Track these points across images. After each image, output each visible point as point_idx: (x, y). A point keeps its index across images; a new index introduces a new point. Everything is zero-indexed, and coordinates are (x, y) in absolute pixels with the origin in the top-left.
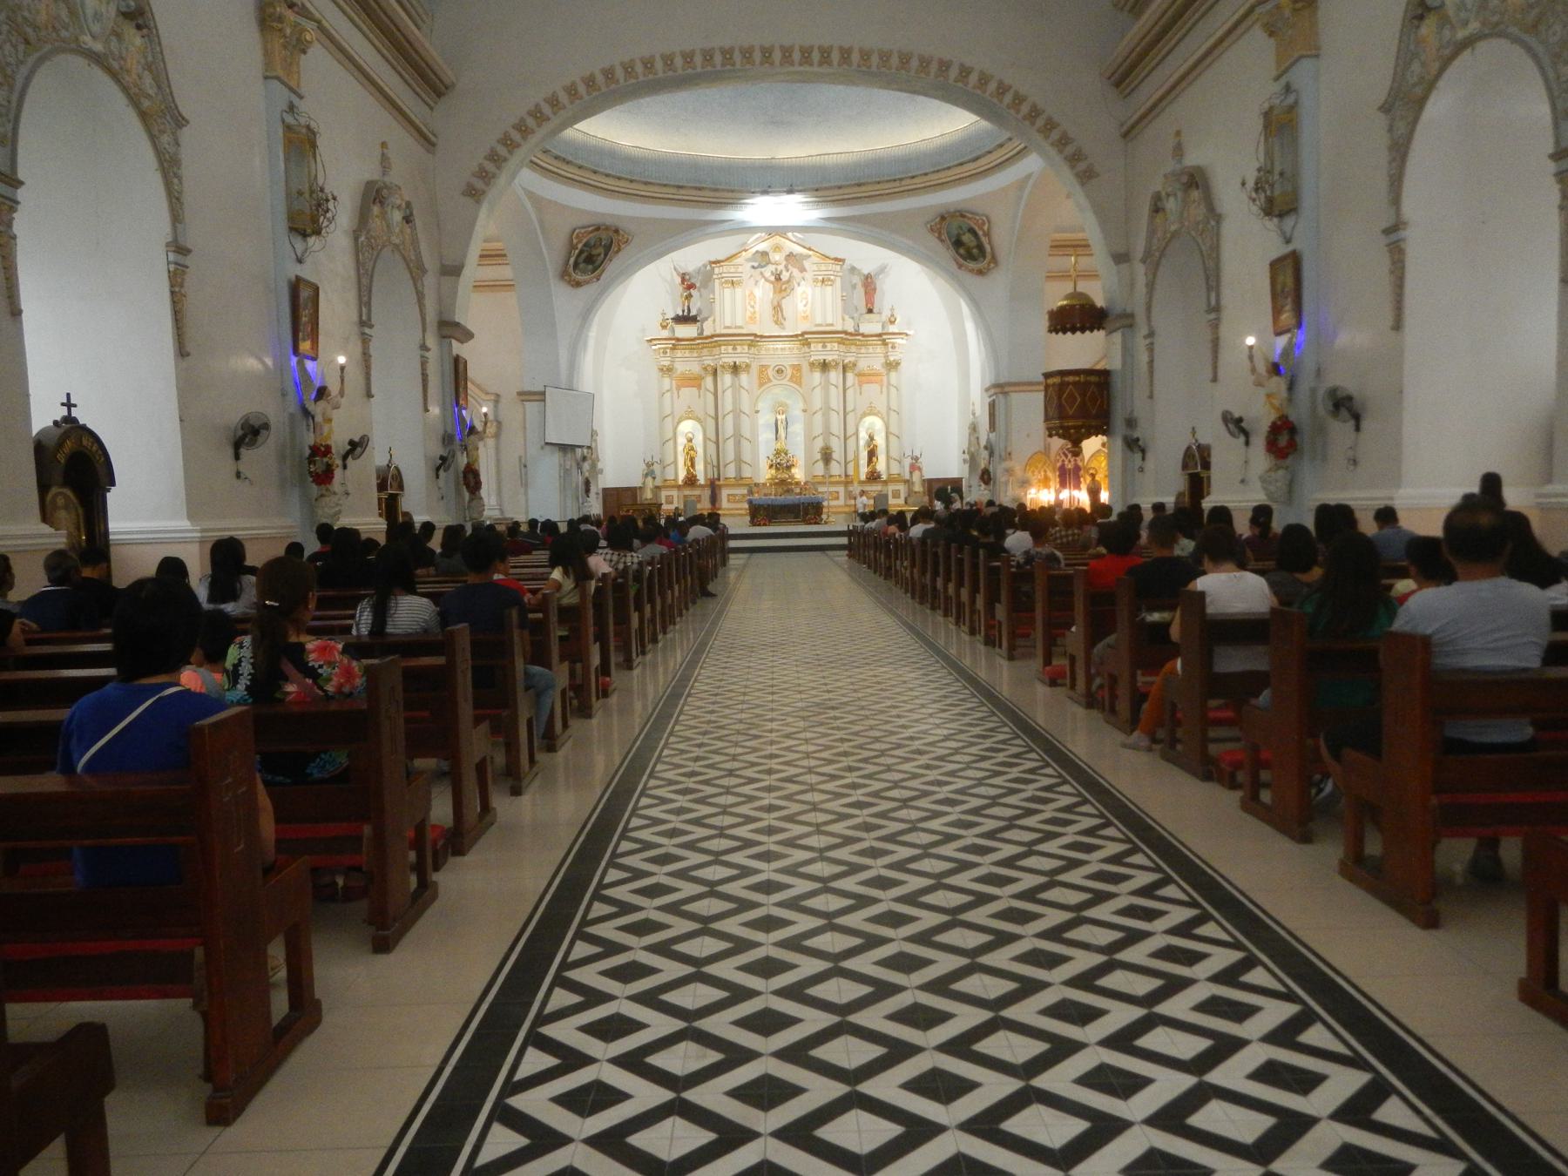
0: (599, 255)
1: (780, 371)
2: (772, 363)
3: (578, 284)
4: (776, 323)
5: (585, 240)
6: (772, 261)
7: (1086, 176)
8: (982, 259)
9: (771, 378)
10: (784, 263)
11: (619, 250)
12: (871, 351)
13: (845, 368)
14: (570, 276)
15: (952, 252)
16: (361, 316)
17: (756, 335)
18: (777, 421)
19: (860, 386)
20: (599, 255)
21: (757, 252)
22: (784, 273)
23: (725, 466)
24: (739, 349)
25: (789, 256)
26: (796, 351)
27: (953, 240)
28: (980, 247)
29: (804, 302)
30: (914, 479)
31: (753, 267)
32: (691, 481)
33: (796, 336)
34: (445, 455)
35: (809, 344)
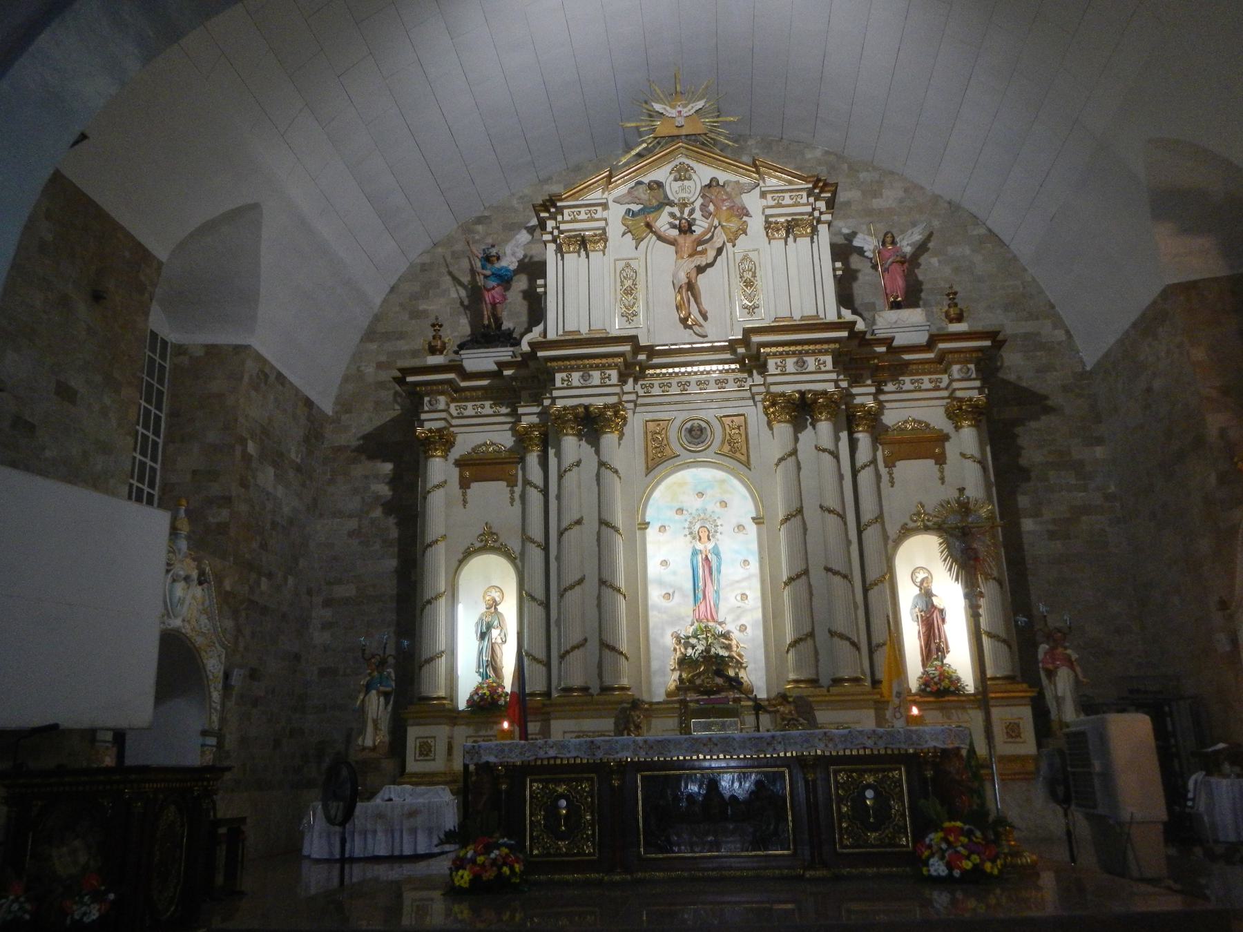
1: (696, 434)
2: (678, 417)
4: (684, 321)
6: (671, 198)
9: (676, 447)
10: (700, 201)
12: (908, 386)
17: (633, 339)
18: (695, 553)
19: (890, 464)
21: (640, 183)
22: (697, 215)
23: (562, 657)
24: (596, 376)
25: (709, 186)
26: (732, 386)
30: (1060, 694)
33: (732, 345)
35: (763, 369)
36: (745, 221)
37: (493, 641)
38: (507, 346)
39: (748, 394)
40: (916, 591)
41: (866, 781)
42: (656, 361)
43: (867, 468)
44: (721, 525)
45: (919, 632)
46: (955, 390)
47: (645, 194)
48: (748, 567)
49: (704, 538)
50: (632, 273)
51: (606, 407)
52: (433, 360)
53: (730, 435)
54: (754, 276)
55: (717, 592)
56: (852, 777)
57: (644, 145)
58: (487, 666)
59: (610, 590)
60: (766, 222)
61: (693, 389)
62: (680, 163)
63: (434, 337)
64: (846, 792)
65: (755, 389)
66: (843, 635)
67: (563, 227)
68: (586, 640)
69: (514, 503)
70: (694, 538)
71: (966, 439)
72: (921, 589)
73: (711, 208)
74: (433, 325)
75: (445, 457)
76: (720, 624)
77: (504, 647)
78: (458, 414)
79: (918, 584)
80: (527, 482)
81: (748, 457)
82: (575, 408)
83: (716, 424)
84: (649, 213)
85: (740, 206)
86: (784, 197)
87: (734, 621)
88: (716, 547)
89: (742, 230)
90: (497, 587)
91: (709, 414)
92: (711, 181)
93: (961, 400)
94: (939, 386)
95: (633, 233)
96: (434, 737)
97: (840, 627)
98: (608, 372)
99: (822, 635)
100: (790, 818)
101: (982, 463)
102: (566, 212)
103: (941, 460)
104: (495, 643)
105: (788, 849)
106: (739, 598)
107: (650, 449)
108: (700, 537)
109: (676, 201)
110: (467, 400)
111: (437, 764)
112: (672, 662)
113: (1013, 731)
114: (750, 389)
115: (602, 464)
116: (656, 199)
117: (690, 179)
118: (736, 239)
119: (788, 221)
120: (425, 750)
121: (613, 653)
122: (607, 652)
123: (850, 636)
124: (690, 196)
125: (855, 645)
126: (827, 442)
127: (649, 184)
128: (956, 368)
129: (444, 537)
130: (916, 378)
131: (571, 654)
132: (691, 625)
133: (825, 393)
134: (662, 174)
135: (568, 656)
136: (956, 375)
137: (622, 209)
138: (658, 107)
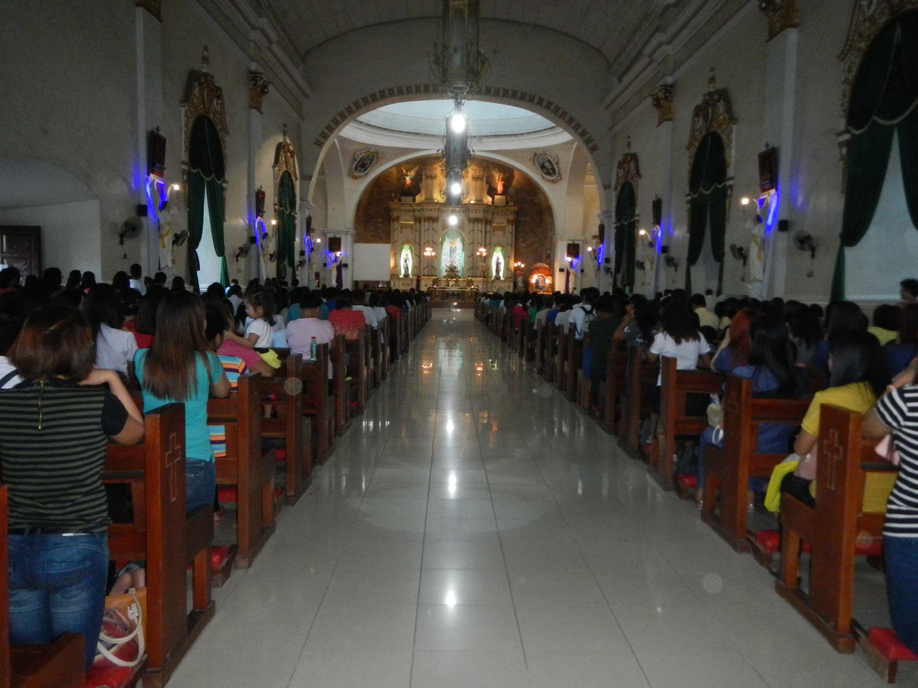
0: (367, 163)
3: (356, 178)
5: (361, 156)
7: (593, 150)
8: (553, 175)
11: (376, 163)
13: (486, 223)
14: (352, 173)
15: (540, 170)
16: (274, 200)
18: (451, 247)
19: (494, 231)
20: (367, 163)
27: (541, 164)
28: (553, 169)
32: (406, 276)
34: (301, 260)
40: (496, 258)
71: (510, 228)
75: (397, 222)
80: (416, 230)
82: (428, 217)
99: (475, 267)
101: (512, 234)
103: (504, 231)
112: (444, 270)
113: (509, 287)
115: (433, 229)
120: (395, 286)
122: (433, 269)
126: (480, 229)
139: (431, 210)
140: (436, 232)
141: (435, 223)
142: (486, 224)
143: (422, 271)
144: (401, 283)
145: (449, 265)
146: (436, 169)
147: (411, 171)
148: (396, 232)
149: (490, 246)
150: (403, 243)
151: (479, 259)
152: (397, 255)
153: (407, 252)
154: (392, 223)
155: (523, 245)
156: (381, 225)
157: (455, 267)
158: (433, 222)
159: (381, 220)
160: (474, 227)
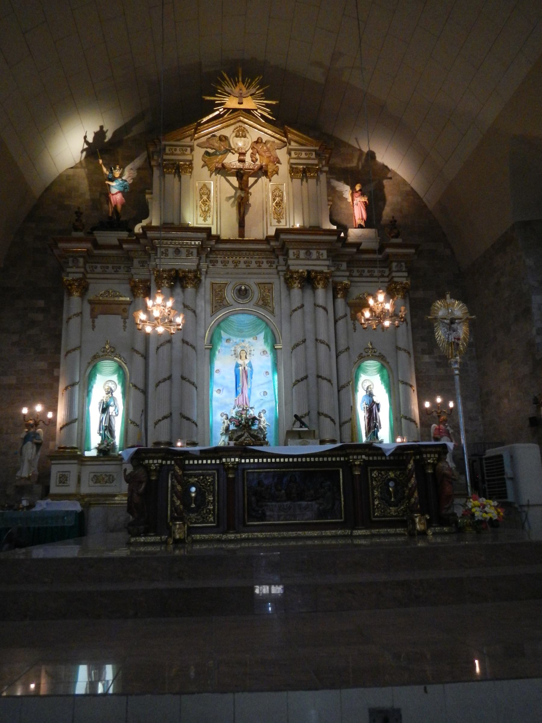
6: (233, 147)
10: (250, 151)
12: (366, 273)
17: (208, 230)
18: (237, 366)
21: (214, 136)
23: (156, 424)
25: (257, 142)
26: (265, 265)
29: (277, 199)
31: (207, 153)
33: (268, 239)
36: (277, 166)
37: (110, 414)
38: (123, 231)
39: (275, 271)
40: (364, 393)
41: (390, 476)
42: (221, 246)
43: (342, 320)
44: (254, 350)
45: (365, 417)
46: (393, 277)
47: (217, 143)
48: (268, 376)
49: (243, 357)
50: (207, 191)
51: (190, 272)
52: (75, 234)
53: (263, 295)
54: (282, 200)
55: (250, 389)
56: (381, 474)
57: (217, 113)
58: (105, 430)
59: (188, 384)
60: (291, 167)
61: (242, 265)
62: (240, 126)
63: (77, 220)
64: (377, 482)
65: (280, 268)
66: (326, 415)
67: (165, 157)
68: (171, 414)
69: (126, 329)
70: (237, 357)
72: (367, 392)
73: (257, 156)
74: (76, 213)
76: (252, 408)
77: (116, 418)
78: (91, 271)
79: (366, 389)
81: (273, 308)
82: (170, 270)
83: (255, 288)
84: (219, 155)
85: (275, 156)
86: (302, 153)
87: (258, 407)
88: (250, 361)
89: (276, 171)
90: (113, 381)
91: (252, 282)
92: (258, 139)
93: (396, 283)
94: (383, 275)
95: (209, 165)
96: (69, 472)
97: (325, 409)
98: (191, 250)
100: (342, 499)
102: (167, 149)
104: (112, 415)
105: (341, 518)
106: (262, 394)
107: (214, 299)
108: (241, 357)
109: (236, 150)
110: (98, 263)
111: (71, 489)
112: (222, 430)
114: (277, 268)
116: (224, 147)
117: (245, 137)
118: (272, 177)
119: (304, 169)
120: (63, 479)
121: (188, 421)
123: (330, 415)
124: (245, 147)
125: (332, 420)
127: (220, 137)
128: (394, 264)
129: (80, 347)
130: (370, 269)
131: (162, 422)
132: (234, 409)
133: (322, 272)
134: (228, 132)
135: (160, 423)
136: (394, 269)
137: (203, 150)
138: (227, 88)
139: (177, 251)
140: (194, 312)
141: (190, 289)
142: (335, 297)
143: (151, 424)
144: (87, 472)
145: (234, 415)
146: (192, 150)
147: (123, 167)
148: (75, 322)
149: (350, 356)
150: (96, 358)
151: (325, 381)
152: (77, 387)
153: (112, 386)
154: (66, 298)
155: (426, 358)
156: (40, 317)
157: (254, 419)
158: (183, 288)
159: (41, 303)
160: (303, 297)
